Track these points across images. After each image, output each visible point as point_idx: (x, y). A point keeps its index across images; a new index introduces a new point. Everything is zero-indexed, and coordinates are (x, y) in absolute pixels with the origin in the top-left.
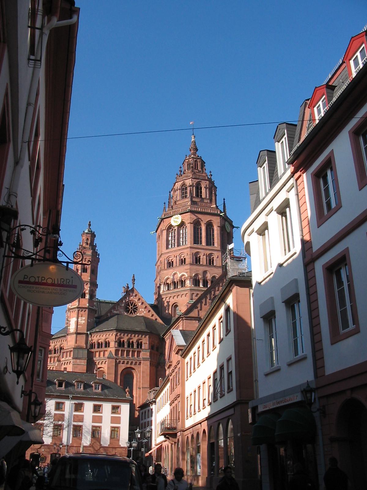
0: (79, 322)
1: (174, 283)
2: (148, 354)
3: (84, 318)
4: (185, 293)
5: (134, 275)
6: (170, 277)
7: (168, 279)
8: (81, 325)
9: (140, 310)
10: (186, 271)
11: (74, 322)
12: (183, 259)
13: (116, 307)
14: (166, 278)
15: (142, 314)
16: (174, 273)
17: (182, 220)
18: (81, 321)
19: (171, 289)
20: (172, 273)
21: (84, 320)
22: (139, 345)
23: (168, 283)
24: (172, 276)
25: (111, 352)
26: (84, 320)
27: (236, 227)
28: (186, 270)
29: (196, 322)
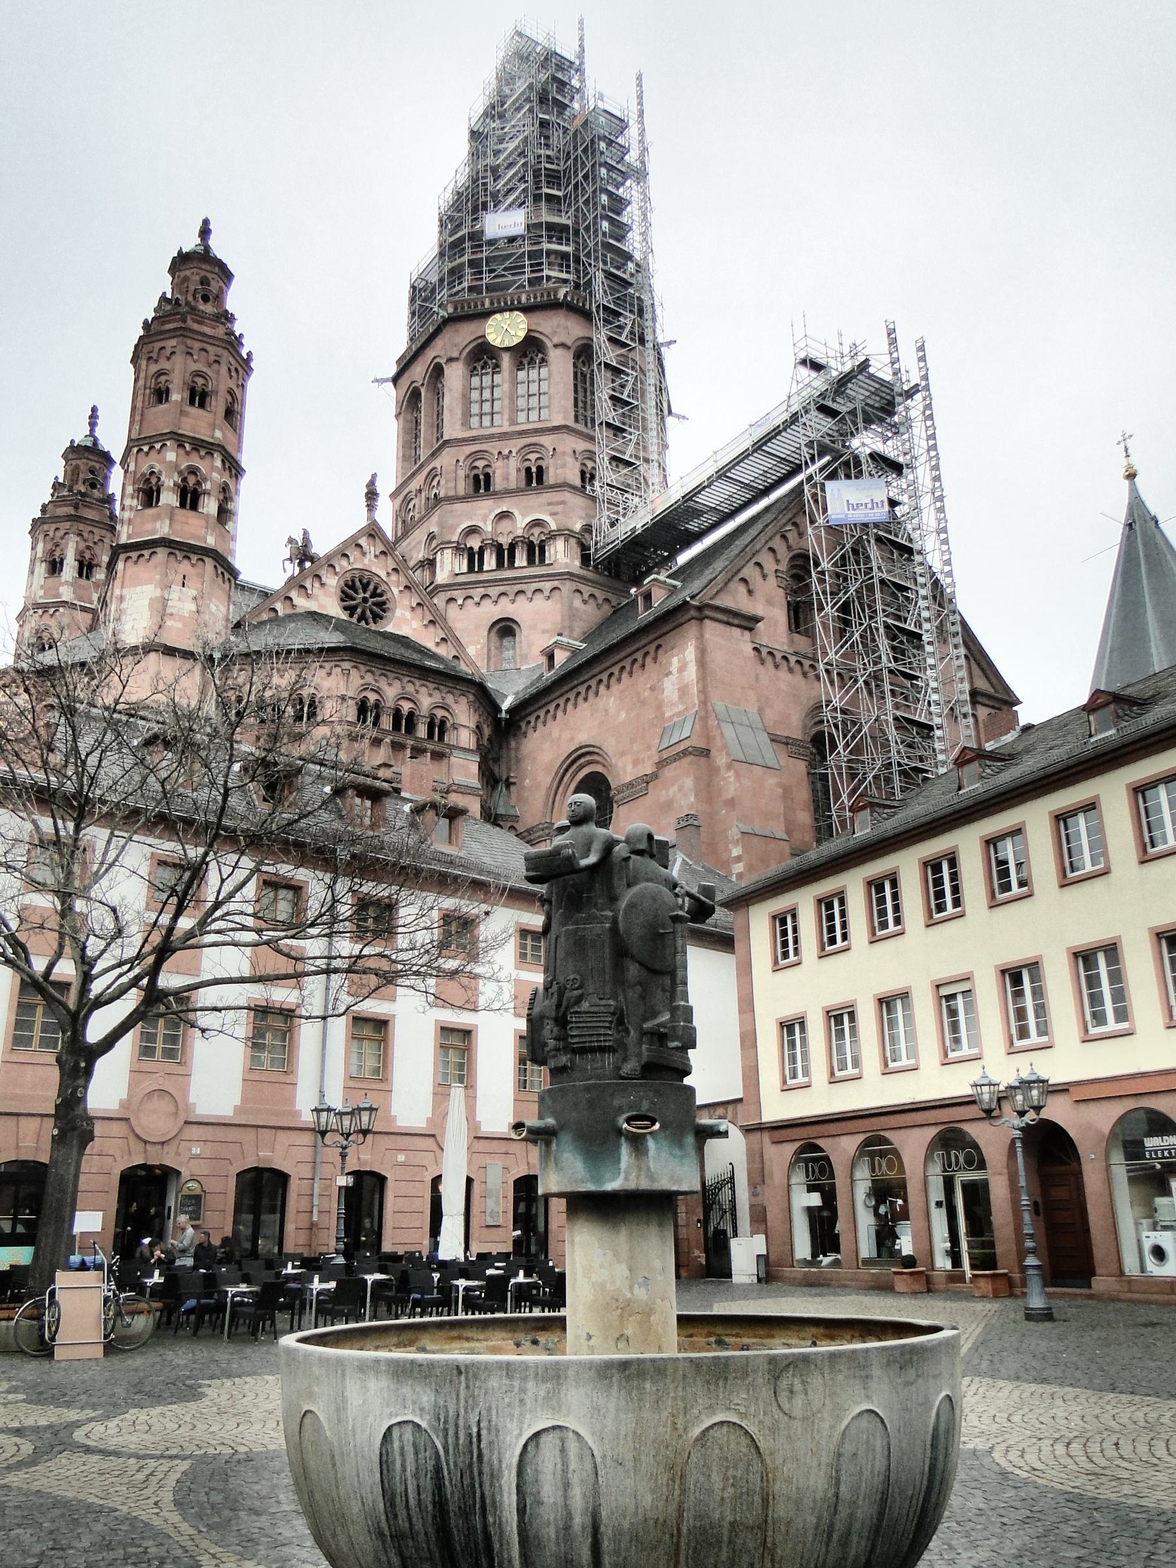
1: (499, 549)
2: (474, 768)
5: (374, 476)
6: (481, 524)
7: (472, 530)
10: (550, 507)
11: (147, 602)
12: (534, 470)
13: (308, 586)
16: (497, 512)
17: (529, 330)
20: (491, 511)
22: (439, 728)
24: (489, 523)
27: (678, 417)
28: (550, 504)
29: (742, 635)
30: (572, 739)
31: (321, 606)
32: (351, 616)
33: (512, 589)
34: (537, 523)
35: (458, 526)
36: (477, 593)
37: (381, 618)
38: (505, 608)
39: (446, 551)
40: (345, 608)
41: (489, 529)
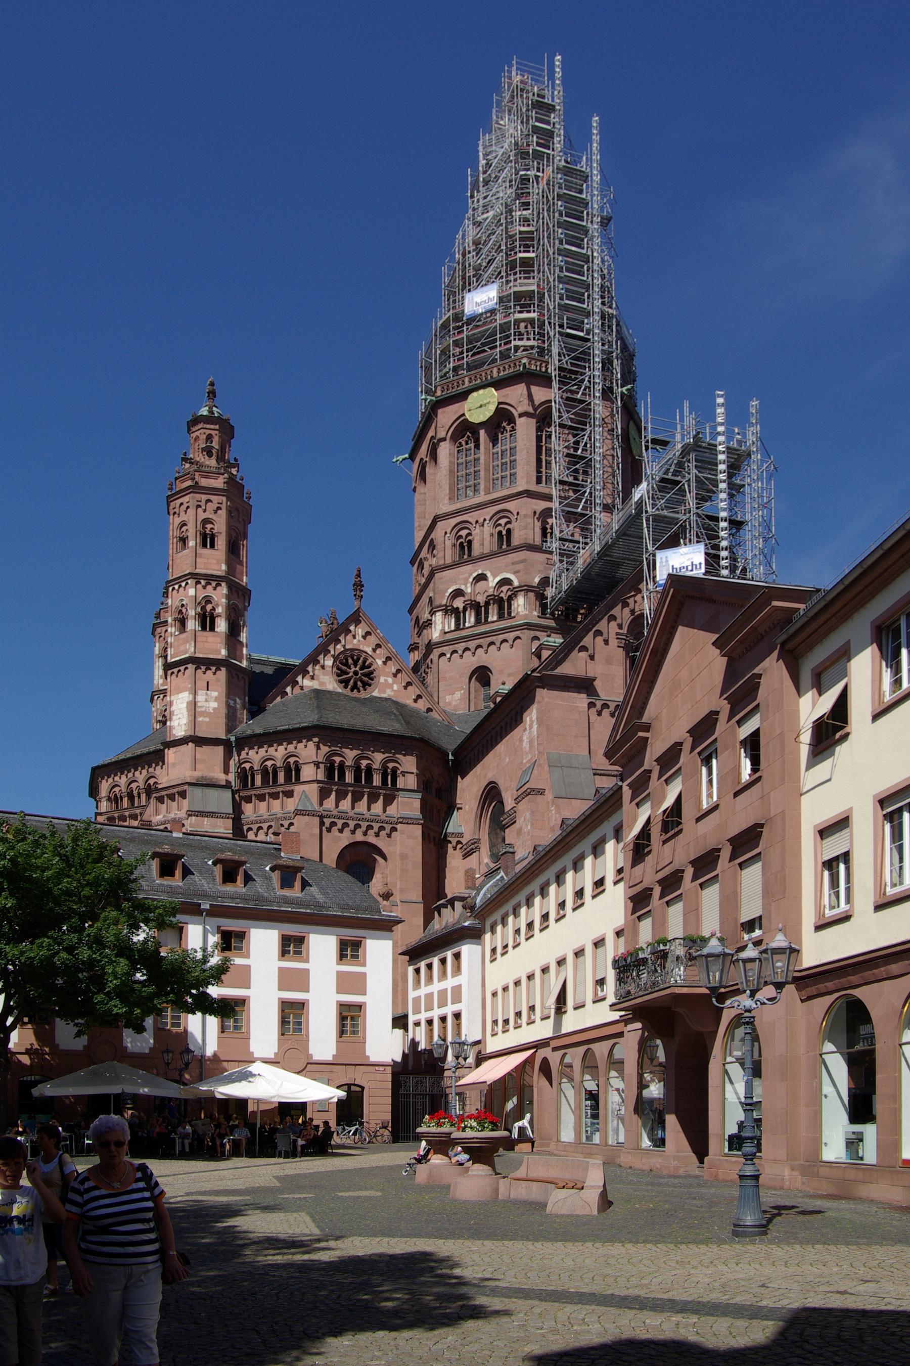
0: (199, 704)
2: (417, 804)
3: (215, 694)
4: (511, 636)
6: (463, 587)
7: (458, 593)
8: (204, 714)
9: (382, 680)
14: (450, 591)
15: (388, 693)
18: (206, 701)
19: (467, 625)
20: (470, 575)
21: (216, 699)
22: (390, 775)
23: (458, 608)
24: (469, 585)
25: (306, 796)
26: (216, 699)
30: (485, 776)
31: (321, 684)
32: (346, 687)
33: (484, 642)
34: (506, 582)
35: (446, 591)
36: (460, 647)
37: (370, 685)
38: (480, 658)
39: (438, 614)
40: (341, 682)
41: (469, 590)
